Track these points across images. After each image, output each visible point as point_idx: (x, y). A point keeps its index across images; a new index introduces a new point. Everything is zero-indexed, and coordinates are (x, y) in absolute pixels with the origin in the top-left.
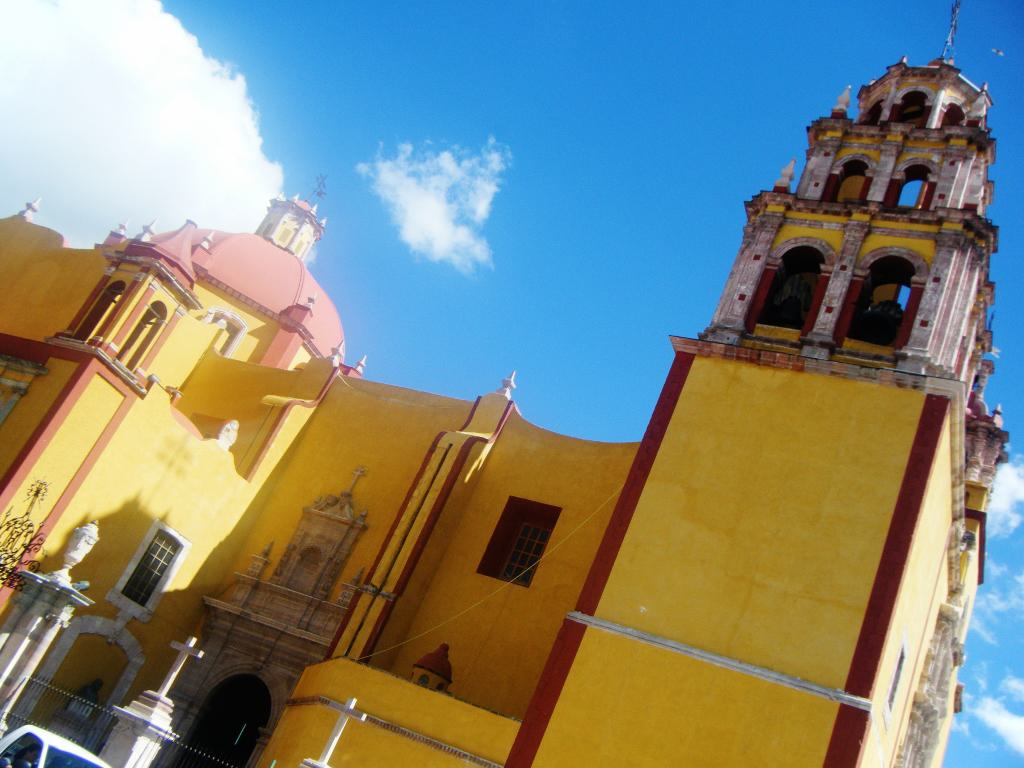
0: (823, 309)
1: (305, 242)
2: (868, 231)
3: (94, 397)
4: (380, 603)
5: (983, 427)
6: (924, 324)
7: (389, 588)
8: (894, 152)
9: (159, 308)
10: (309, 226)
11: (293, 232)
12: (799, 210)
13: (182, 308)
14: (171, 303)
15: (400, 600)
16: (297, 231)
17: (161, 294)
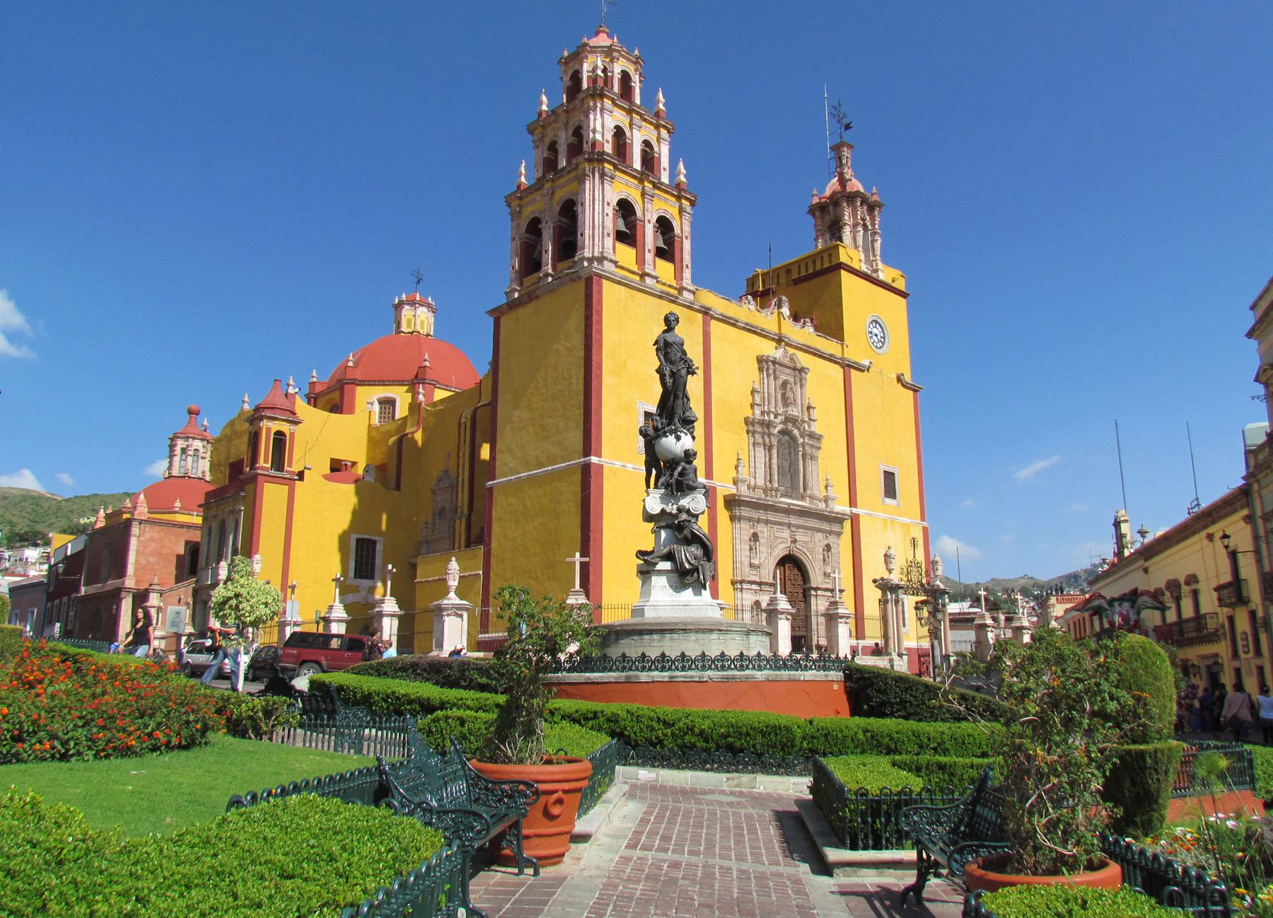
1: (424, 319)
2: (553, 193)
3: (272, 496)
4: (464, 521)
5: (841, 197)
6: (582, 235)
8: (563, 127)
10: (421, 308)
13: (293, 427)
14: (285, 428)
15: (472, 514)
16: (414, 316)
17: (275, 426)
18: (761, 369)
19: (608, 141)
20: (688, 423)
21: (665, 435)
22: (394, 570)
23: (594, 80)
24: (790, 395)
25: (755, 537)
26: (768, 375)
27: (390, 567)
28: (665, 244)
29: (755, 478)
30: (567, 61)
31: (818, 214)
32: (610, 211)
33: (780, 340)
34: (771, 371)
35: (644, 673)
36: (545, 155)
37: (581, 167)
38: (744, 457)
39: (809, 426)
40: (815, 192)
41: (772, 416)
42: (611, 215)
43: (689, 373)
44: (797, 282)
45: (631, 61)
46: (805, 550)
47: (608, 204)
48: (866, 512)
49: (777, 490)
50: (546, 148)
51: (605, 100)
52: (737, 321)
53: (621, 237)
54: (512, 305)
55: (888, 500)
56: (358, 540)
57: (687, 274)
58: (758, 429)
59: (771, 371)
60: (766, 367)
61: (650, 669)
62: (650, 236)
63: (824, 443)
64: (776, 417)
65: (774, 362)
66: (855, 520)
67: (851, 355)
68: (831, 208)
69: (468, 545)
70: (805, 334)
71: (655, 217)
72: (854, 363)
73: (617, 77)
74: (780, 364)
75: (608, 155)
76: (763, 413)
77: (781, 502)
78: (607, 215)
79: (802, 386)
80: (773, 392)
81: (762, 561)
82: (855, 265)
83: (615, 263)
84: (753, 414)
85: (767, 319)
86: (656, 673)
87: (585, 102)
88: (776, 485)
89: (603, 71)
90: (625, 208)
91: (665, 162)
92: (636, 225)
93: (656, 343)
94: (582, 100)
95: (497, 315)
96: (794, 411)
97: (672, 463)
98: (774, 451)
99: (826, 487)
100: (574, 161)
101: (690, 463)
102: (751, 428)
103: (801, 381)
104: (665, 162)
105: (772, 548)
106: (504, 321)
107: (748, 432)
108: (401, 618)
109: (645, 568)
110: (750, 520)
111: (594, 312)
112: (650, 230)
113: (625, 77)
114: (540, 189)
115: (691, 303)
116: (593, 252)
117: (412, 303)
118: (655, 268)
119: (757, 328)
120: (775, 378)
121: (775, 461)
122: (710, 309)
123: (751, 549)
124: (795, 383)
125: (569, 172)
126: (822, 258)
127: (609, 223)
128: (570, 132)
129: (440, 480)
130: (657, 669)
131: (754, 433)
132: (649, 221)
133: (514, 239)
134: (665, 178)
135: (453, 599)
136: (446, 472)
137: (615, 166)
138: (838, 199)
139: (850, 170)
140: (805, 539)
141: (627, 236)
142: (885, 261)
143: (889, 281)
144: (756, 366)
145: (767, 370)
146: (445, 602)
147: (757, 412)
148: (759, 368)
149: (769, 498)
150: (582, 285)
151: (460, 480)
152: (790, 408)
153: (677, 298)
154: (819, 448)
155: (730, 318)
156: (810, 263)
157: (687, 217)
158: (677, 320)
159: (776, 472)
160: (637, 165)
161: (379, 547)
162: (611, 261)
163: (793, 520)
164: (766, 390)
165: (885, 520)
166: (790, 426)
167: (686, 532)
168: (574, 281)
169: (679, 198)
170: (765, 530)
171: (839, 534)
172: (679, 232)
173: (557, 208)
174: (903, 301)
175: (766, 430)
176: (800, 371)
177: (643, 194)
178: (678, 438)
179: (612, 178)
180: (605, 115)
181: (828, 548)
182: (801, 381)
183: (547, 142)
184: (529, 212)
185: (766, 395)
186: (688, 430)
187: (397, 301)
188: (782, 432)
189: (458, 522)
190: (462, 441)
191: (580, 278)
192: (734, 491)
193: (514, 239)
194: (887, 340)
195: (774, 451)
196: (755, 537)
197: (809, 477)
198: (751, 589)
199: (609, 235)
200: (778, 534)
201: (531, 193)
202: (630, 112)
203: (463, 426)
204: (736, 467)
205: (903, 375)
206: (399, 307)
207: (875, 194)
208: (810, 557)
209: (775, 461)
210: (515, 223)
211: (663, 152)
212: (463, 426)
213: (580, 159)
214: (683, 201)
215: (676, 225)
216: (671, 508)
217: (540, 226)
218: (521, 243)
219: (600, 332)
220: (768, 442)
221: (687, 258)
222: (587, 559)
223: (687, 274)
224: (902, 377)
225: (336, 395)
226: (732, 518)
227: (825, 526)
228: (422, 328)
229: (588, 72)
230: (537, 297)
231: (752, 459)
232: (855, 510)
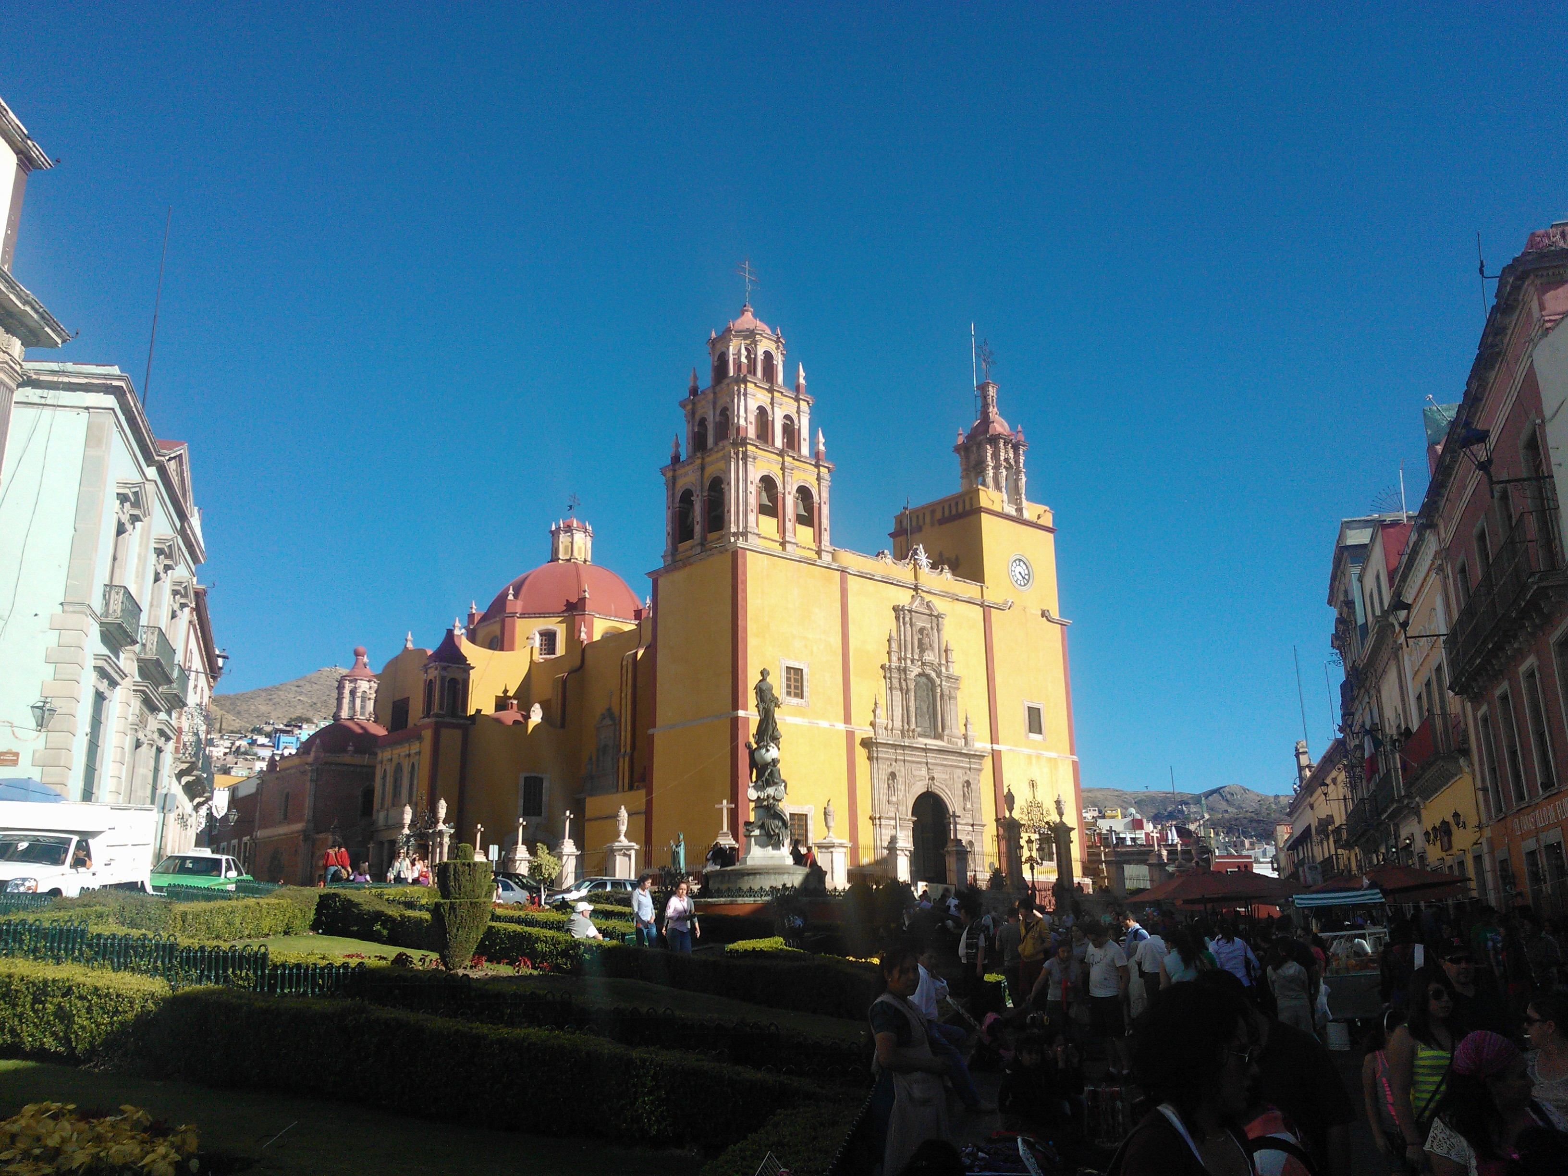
0: (695, 523)
2: (703, 468)
4: (627, 759)
7: (629, 750)
9: (454, 681)
11: (570, 544)
12: (679, 469)
16: (572, 543)
18: (897, 618)
19: (751, 423)
20: (775, 739)
21: (759, 748)
22: (572, 816)
23: (738, 366)
24: (926, 640)
25: (893, 775)
26: (904, 623)
27: (568, 813)
28: (805, 512)
29: (892, 720)
30: (714, 343)
31: (963, 453)
32: (752, 489)
33: (916, 589)
34: (907, 619)
35: (740, 899)
36: (696, 430)
37: (727, 449)
38: (882, 702)
39: (947, 670)
40: (961, 432)
41: (909, 662)
42: (754, 492)
43: (776, 706)
44: (942, 521)
45: (773, 340)
46: (944, 787)
47: (752, 483)
48: (1009, 747)
49: (913, 731)
50: (696, 423)
51: (749, 384)
52: (874, 576)
53: (763, 510)
54: (668, 569)
55: (1030, 734)
56: (526, 779)
57: (826, 537)
58: (895, 675)
59: (907, 619)
60: (902, 616)
61: (743, 896)
62: (791, 505)
63: (963, 685)
64: (912, 661)
65: (910, 611)
66: (996, 756)
67: (991, 596)
68: (975, 449)
69: (631, 788)
70: (945, 579)
71: (795, 488)
72: (997, 604)
73: (760, 356)
74: (916, 612)
75: (751, 439)
76: (899, 659)
77: (917, 743)
78: (751, 492)
79: (938, 631)
80: (909, 639)
81: (900, 798)
82: (997, 508)
83: (758, 535)
84: (890, 661)
85: (903, 571)
86: (746, 899)
87: (731, 386)
88: (913, 726)
89: (746, 357)
90: (768, 483)
91: (805, 433)
92: (777, 497)
93: (755, 688)
94: (728, 385)
95: (655, 577)
96: (929, 657)
97: (766, 765)
98: (912, 694)
99: (965, 725)
100: (721, 444)
101: (775, 766)
102: (888, 675)
103: (938, 625)
104: (805, 433)
105: (909, 786)
106: (661, 582)
107: (885, 677)
108: (577, 856)
109: (747, 833)
110: (887, 759)
111: (739, 581)
112: (790, 501)
113: (768, 355)
114: (692, 463)
115: (828, 564)
116: (738, 527)
117: (569, 529)
118: (795, 535)
119: (894, 579)
120: (911, 625)
121: (912, 704)
122: (847, 568)
123: (889, 787)
124: (932, 627)
125: (717, 452)
126: (964, 502)
127: (753, 501)
128: (718, 412)
129: (603, 717)
130: (747, 896)
131: (890, 678)
132: (789, 493)
133: (669, 508)
134: (805, 450)
135: (624, 841)
136: (609, 710)
137: (757, 447)
138: (981, 441)
139: (996, 409)
140: (944, 776)
141: (771, 509)
142: (1027, 499)
143: (1034, 519)
144: (893, 614)
145: (904, 618)
146: (617, 844)
147: (894, 658)
148: (896, 617)
149: (906, 740)
150: (728, 557)
151: (623, 720)
152: (926, 653)
153: (816, 561)
154: (958, 689)
155: (868, 574)
156: (953, 504)
157: (825, 484)
158: (768, 674)
159: (914, 714)
160: (779, 442)
161: (545, 785)
162: (754, 534)
163: (932, 758)
164: (902, 637)
165: (1030, 756)
166: (928, 671)
167: (772, 812)
168: (722, 553)
169: (817, 466)
170: (903, 769)
171: (980, 770)
172: (818, 498)
173: (707, 484)
174: (1051, 536)
175: (902, 674)
176: (937, 618)
177: (783, 469)
178: (768, 751)
179: (754, 458)
180: (748, 399)
181: (968, 783)
182: (938, 625)
183: (698, 417)
184: (683, 483)
185: (903, 642)
186: (776, 745)
187: (553, 528)
188: (920, 675)
189: (621, 760)
190: (624, 685)
191: (727, 550)
192: (872, 734)
193: (669, 508)
194: (1031, 577)
195: (912, 694)
196: (893, 775)
197: (947, 718)
198: (890, 825)
199: (752, 511)
200: (916, 773)
201: (684, 467)
202: (771, 391)
203: (624, 669)
204: (874, 711)
205: (1048, 611)
206: (555, 534)
207: (1020, 432)
208: (949, 793)
209: (912, 704)
210: (670, 493)
211: (804, 425)
212: (624, 669)
213: (726, 443)
214: (822, 469)
215: (815, 492)
216: (762, 795)
217: (692, 498)
218: (674, 513)
219: (745, 599)
220: (904, 687)
221: (825, 523)
222: (733, 806)
223: (826, 537)
224: (1047, 614)
225: (496, 628)
226: (870, 758)
227: (964, 763)
228: (580, 553)
229: (733, 354)
230: (690, 564)
231: (889, 703)
232: (996, 747)
